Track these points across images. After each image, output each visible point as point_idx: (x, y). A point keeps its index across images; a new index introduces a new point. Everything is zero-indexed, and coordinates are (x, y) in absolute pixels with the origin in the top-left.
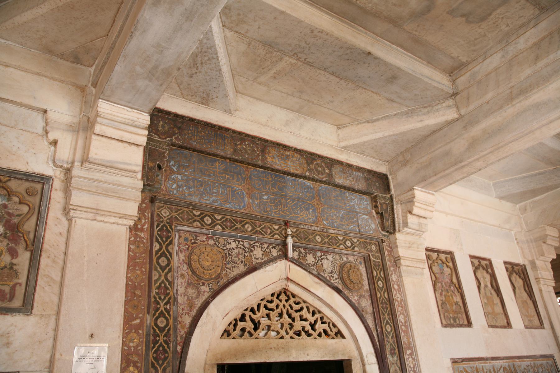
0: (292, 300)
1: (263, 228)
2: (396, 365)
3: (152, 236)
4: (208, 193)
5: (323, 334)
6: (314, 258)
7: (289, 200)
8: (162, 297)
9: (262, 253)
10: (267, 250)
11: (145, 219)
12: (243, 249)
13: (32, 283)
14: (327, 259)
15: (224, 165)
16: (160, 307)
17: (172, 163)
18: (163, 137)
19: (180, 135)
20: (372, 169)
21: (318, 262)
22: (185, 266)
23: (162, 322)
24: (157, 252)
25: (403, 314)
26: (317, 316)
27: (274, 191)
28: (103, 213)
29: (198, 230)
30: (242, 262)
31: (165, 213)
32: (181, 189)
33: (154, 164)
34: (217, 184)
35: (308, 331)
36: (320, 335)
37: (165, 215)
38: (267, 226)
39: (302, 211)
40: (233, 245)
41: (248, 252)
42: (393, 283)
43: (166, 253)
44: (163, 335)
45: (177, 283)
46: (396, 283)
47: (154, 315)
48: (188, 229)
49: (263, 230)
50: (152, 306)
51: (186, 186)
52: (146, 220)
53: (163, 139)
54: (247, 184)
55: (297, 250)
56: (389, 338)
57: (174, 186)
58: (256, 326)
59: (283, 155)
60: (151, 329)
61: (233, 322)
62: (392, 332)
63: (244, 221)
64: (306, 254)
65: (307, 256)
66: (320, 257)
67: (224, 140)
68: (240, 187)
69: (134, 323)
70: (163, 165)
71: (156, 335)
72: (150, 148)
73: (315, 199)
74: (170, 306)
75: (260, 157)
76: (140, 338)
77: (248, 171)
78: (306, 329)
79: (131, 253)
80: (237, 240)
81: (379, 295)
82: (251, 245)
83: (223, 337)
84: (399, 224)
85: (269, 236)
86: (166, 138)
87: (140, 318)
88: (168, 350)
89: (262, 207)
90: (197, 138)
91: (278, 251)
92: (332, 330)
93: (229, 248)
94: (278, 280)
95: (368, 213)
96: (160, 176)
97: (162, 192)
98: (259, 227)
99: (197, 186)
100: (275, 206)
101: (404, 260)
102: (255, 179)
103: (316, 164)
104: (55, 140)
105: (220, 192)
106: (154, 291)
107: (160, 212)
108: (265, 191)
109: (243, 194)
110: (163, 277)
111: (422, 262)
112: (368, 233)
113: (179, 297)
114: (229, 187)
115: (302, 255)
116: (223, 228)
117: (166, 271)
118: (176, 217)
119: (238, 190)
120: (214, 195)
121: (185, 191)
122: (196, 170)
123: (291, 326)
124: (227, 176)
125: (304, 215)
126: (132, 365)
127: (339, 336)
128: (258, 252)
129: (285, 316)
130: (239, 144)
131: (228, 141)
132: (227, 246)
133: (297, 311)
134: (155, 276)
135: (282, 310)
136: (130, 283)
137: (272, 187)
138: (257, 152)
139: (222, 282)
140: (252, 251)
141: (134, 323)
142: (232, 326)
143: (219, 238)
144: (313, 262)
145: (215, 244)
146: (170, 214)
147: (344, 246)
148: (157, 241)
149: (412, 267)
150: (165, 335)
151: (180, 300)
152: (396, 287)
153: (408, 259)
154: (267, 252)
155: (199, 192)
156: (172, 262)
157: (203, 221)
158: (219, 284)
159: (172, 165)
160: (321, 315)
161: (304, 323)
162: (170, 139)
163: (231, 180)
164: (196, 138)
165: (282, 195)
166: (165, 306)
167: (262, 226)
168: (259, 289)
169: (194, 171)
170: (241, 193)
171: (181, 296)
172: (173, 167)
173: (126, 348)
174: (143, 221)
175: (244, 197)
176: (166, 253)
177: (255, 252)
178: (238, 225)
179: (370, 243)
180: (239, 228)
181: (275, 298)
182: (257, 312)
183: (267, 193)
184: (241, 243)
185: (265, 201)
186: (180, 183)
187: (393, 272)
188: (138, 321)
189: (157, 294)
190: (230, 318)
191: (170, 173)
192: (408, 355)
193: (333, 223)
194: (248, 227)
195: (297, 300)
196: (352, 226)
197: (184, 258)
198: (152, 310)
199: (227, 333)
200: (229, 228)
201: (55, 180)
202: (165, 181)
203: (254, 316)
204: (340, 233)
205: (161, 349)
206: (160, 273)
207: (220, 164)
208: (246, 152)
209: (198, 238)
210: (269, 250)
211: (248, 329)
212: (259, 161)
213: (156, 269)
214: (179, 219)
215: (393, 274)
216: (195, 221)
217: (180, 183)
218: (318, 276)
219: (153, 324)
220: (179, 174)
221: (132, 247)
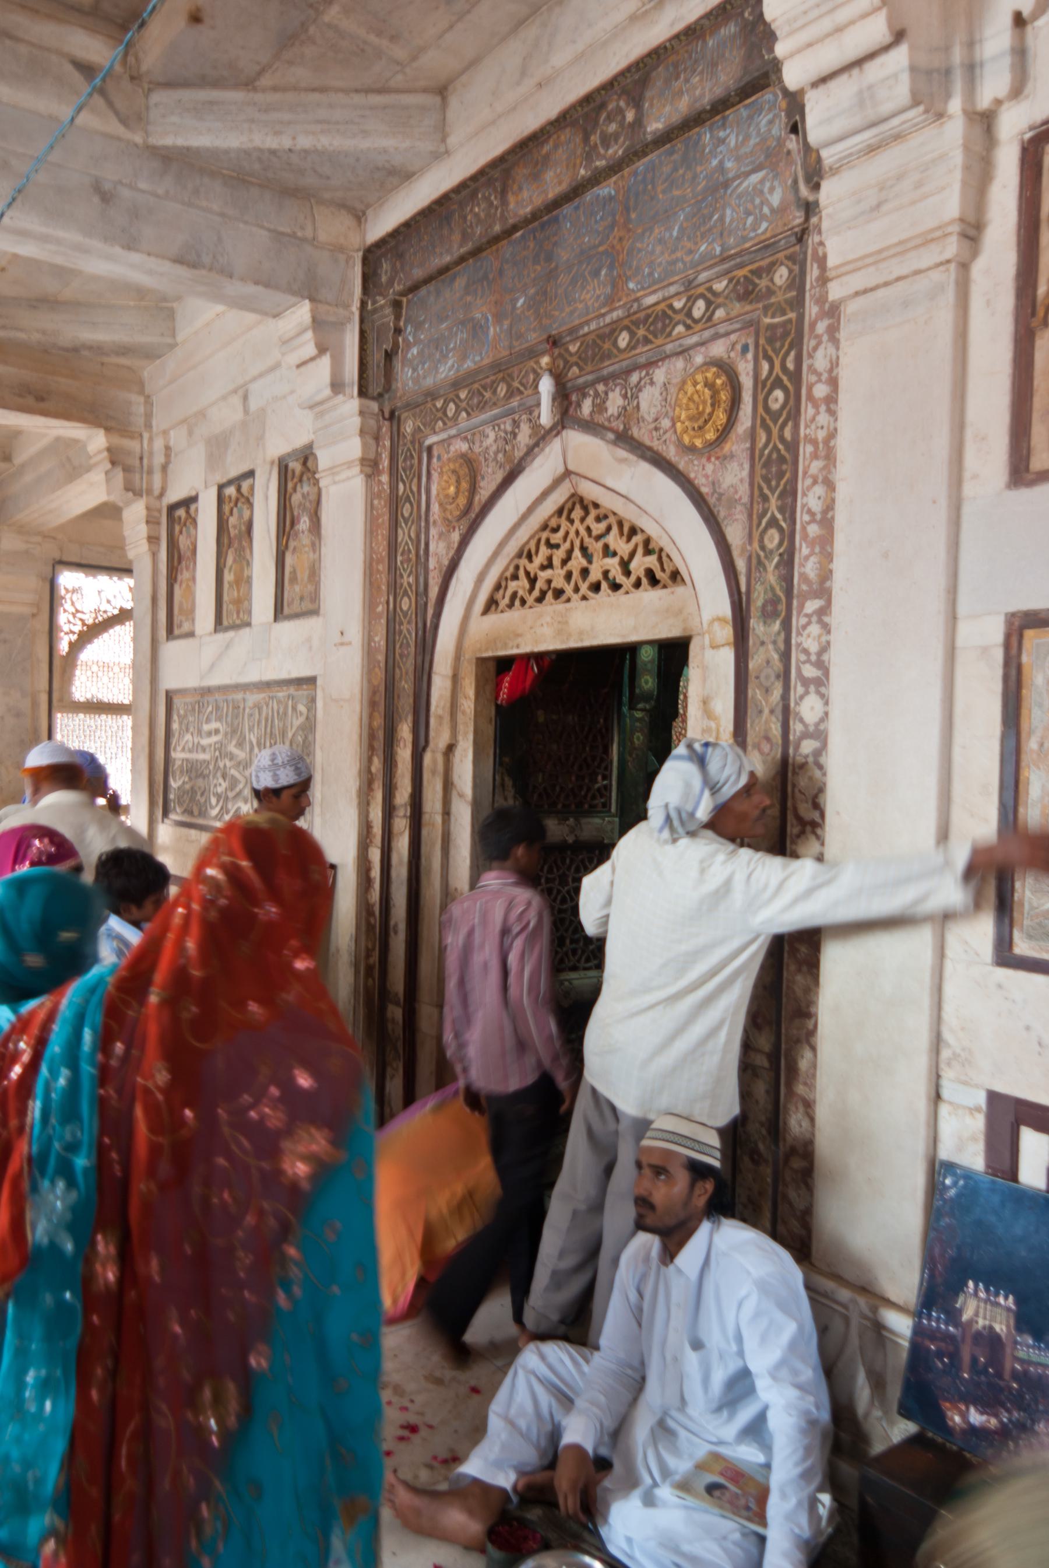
0: (593, 513)
2: (771, 647)
26: (638, 539)
36: (638, 584)
56: (765, 569)
78: (611, 575)
92: (666, 567)
111: (932, 240)
112: (752, 239)
123: (585, 572)
129: (577, 553)
152: (821, 391)
153: (860, 264)
192: (807, 615)
195: (601, 511)
196: (703, 248)
199: (491, 604)
204: (673, 290)
215: (823, 346)
218: (624, 439)
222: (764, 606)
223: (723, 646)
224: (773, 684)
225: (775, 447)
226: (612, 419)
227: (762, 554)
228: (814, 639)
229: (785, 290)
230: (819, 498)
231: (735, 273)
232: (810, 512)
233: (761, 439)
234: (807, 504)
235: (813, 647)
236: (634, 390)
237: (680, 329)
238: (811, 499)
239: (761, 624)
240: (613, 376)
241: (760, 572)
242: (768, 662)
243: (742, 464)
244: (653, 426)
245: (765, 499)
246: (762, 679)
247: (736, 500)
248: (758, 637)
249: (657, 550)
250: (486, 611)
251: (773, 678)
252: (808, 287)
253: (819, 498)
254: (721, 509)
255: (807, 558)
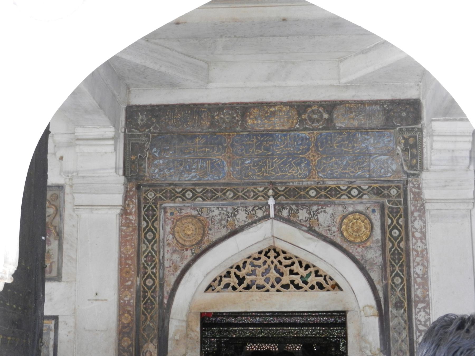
0: (282, 255)
1: (245, 192)
2: (400, 318)
3: (139, 217)
4: (187, 170)
5: (316, 287)
6: (308, 213)
7: (277, 159)
8: (150, 263)
9: (246, 215)
10: (252, 212)
11: (133, 204)
12: (227, 215)
13: (60, 261)
14: (325, 212)
15: (204, 138)
16: (148, 271)
17: (155, 149)
18: (143, 130)
19: (157, 123)
20: (394, 98)
21: (312, 217)
22: (171, 236)
23: (149, 282)
24: (144, 229)
25: (423, 265)
26: (311, 269)
27: (259, 153)
28: (96, 208)
29: (181, 205)
30: (224, 227)
31: (151, 195)
32: (162, 173)
33: (136, 157)
34: (196, 160)
35: (298, 284)
36: (312, 288)
37: (151, 197)
38: (250, 190)
39: (292, 168)
40: (217, 212)
41: (231, 217)
42: (414, 230)
43: (153, 228)
44: (150, 291)
45: (164, 251)
46: (419, 230)
47: (143, 277)
48: (172, 205)
49: (246, 194)
50: (142, 271)
51: (167, 168)
52: (134, 205)
53: (143, 131)
54: (228, 152)
55: (288, 207)
56: (395, 290)
57: (156, 171)
58: (241, 280)
59: (267, 112)
60: (142, 288)
61: (219, 279)
62: (402, 285)
63: (226, 189)
64: (298, 210)
65: (298, 212)
66: (316, 212)
67: (201, 116)
68: (220, 157)
69: (127, 284)
70: (143, 155)
71: (145, 292)
72: (132, 143)
73: (310, 151)
74: (156, 270)
75: (240, 123)
76: (132, 294)
77: (230, 138)
78: (296, 283)
79: (123, 233)
80: (220, 207)
81: (391, 245)
82: (235, 209)
83: (208, 291)
84: (427, 160)
85: (252, 200)
86: (144, 131)
87: (131, 280)
88: (155, 302)
89: (243, 172)
90: (173, 122)
91: (264, 212)
92: (329, 283)
93: (212, 215)
94: (262, 239)
95: (389, 152)
96: (144, 165)
97: (145, 179)
98: (242, 192)
99: (177, 167)
100: (258, 168)
101: (431, 204)
102: (237, 145)
103: (310, 112)
104: (61, 156)
105: (200, 167)
106: (143, 259)
107: (147, 195)
108: (248, 155)
109: (223, 163)
110: (150, 249)
111: (465, 202)
112: (384, 177)
113: (166, 262)
114: (208, 159)
115: (293, 212)
116: (204, 200)
117: (152, 243)
118: (160, 197)
119: (218, 161)
120: (193, 171)
121: (165, 173)
122: (176, 151)
123: (278, 281)
124: (207, 149)
125: (294, 172)
126: (126, 312)
127: (337, 287)
128: (242, 217)
130: (216, 115)
131: (205, 115)
132: (210, 214)
133: (286, 266)
134: (144, 247)
135: (269, 266)
136: (123, 255)
137: (256, 150)
138: (237, 118)
139: (204, 246)
140: (235, 215)
141: (127, 284)
142: (217, 282)
143: (202, 208)
144: (306, 217)
145: (199, 214)
146: (155, 195)
147: (347, 196)
148: (145, 219)
149: (445, 209)
150: (152, 292)
151: (167, 264)
152: (418, 235)
154: (251, 214)
155: (179, 171)
156: (157, 236)
157: (185, 196)
158: (201, 249)
159: (155, 152)
160: (315, 269)
161: (293, 277)
162: (148, 130)
163: (211, 152)
164: (172, 122)
165: (269, 155)
166: (152, 270)
167: (244, 191)
168: (240, 250)
169: (175, 152)
170: (220, 164)
171: (168, 260)
172: (155, 154)
173: (122, 301)
174: (131, 206)
175: (224, 167)
176: (153, 228)
177: (238, 216)
178: (219, 194)
179: (389, 188)
180: (220, 197)
181: (262, 256)
182: (242, 269)
183: (251, 157)
184: (225, 209)
185: (247, 165)
186: (162, 167)
187: (418, 218)
188: (130, 283)
189: (145, 261)
190: (215, 274)
191: (153, 160)
192: (419, 308)
193: (332, 174)
194: (230, 194)
195: (288, 256)
196: (360, 173)
197: (170, 230)
198: (142, 273)
199: (210, 288)
200: (209, 198)
201: (66, 186)
202: (148, 168)
203: (238, 273)
205: (149, 301)
206: (148, 245)
207: (200, 139)
208: (224, 122)
209: (183, 211)
210: (254, 212)
211: (232, 284)
212: (237, 127)
213: (144, 243)
214: (163, 198)
215: (417, 220)
216: (177, 197)
217: (162, 167)
218: (311, 230)
219: (142, 284)
220: (160, 159)
221: (124, 228)
222: (396, 303)
223: (371, 316)
224: (402, 331)
225: (396, 249)
226: (302, 221)
227: (393, 285)
228: (423, 317)
229: (396, 197)
230: (421, 270)
231: (372, 185)
232: (417, 274)
233: (389, 245)
234: (415, 271)
235: (423, 320)
236: (315, 212)
237: (343, 197)
238: (417, 270)
239: (395, 310)
240: (303, 205)
241: (393, 291)
242: (399, 323)
243: (376, 251)
244: (327, 228)
245: (393, 266)
246: (397, 328)
247: (374, 264)
248: (394, 314)
249: (323, 276)
250: (207, 290)
251: (402, 329)
252: (409, 199)
253: (421, 270)
254: (367, 265)
255: (417, 289)
